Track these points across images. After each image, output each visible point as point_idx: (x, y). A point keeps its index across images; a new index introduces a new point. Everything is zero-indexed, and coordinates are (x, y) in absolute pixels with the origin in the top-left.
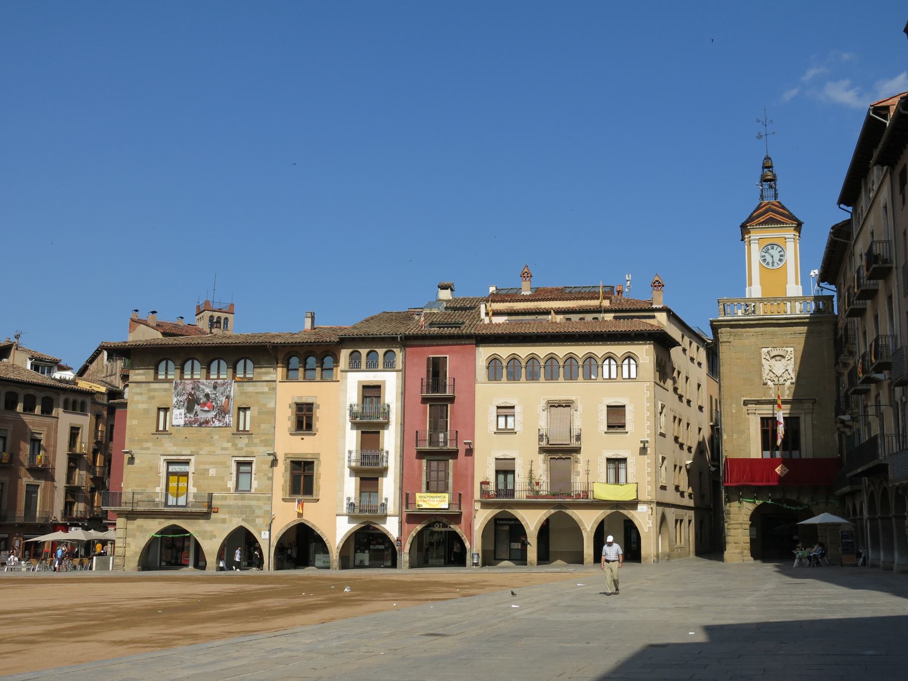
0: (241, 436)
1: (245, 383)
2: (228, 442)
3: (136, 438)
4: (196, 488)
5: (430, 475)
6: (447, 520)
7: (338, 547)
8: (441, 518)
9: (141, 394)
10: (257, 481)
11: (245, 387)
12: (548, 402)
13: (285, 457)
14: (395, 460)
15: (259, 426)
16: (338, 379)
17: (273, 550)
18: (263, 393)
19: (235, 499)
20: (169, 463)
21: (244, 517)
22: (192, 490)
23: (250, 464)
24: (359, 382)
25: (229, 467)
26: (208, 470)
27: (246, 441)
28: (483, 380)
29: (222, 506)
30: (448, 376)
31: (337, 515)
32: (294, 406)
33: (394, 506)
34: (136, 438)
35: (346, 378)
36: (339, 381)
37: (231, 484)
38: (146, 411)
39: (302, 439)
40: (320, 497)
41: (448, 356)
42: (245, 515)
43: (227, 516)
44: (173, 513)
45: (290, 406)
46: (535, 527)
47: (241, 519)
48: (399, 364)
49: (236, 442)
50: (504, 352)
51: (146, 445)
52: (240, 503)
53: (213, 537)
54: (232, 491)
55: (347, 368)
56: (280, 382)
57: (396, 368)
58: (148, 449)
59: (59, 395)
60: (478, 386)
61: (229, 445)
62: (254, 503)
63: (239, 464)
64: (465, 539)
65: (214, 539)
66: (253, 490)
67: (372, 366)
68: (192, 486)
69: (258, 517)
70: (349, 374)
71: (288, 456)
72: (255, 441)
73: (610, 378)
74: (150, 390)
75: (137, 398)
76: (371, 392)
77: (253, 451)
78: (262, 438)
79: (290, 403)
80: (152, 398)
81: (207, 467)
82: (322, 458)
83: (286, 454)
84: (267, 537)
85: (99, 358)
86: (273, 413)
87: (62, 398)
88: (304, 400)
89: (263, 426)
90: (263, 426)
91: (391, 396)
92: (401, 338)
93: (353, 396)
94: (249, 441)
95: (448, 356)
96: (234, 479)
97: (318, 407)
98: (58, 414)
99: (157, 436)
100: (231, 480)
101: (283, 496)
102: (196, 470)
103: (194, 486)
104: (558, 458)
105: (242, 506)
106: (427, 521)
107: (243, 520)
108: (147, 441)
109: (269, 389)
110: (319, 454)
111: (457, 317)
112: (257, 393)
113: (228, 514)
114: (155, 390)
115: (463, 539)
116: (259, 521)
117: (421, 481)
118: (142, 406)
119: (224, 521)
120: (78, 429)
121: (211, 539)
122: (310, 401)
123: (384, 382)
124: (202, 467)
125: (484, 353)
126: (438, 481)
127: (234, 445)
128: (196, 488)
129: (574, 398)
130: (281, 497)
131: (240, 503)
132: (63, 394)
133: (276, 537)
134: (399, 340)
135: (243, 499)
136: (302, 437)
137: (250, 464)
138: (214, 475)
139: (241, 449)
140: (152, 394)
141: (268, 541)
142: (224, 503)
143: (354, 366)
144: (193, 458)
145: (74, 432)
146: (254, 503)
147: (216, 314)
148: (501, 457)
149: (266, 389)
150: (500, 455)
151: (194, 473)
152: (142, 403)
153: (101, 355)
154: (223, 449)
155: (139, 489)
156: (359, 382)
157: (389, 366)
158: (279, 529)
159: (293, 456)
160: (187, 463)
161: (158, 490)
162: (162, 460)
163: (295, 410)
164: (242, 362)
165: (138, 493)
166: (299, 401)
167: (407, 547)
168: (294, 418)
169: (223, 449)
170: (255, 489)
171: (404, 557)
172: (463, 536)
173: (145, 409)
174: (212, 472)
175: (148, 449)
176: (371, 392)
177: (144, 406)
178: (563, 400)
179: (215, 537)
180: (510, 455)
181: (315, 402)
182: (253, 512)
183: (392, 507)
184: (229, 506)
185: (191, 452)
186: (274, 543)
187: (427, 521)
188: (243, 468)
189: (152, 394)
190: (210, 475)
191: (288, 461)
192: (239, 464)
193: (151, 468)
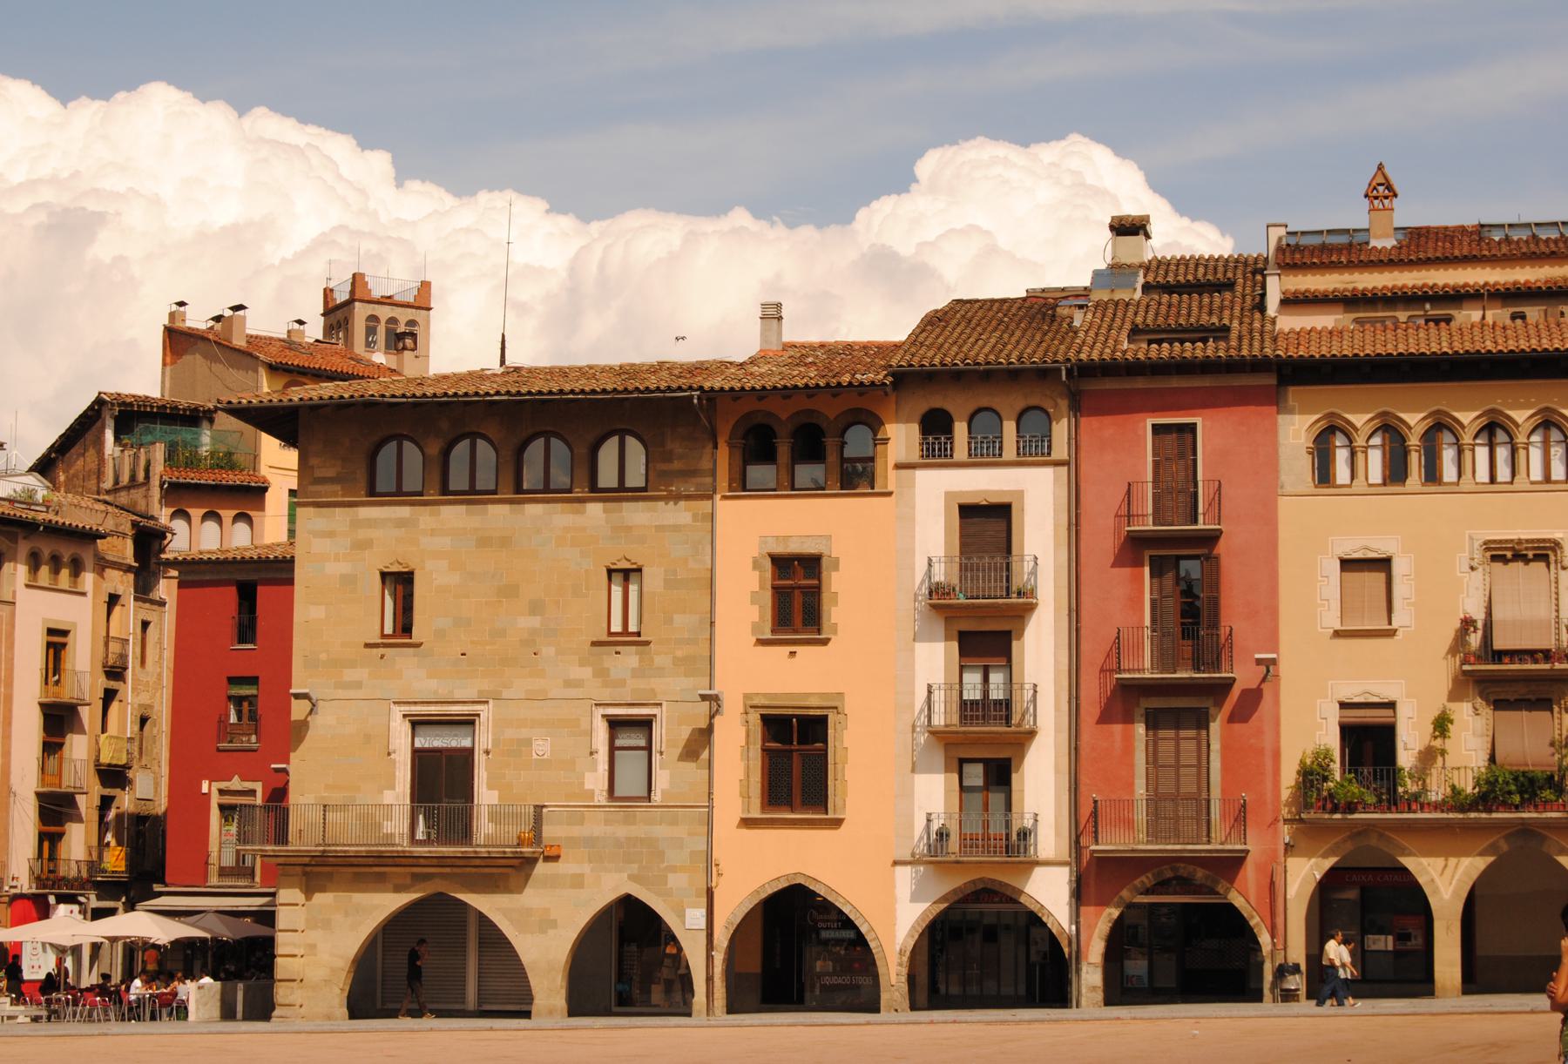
0: (618, 648)
1: (625, 505)
3: (323, 656)
4: (496, 793)
5: (1155, 752)
6: (1207, 872)
7: (901, 950)
8: (1191, 868)
9: (331, 534)
10: (668, 772)
11: (624, 514)
12: (1488, 546)
13: (745, 705)
14: (1057, 709)
15: (669, 621)
16: (890, 489)
17: (719, 957)
18: (676, 528)
19: (607, 822)
21: (636, 872)
23: (645, 724)
24: (949, 495)
25: (590, 733)
26: (528, 742)
28: (1301, 489)
29: (574, 842)
30: (1200, 477)
31: (895, 863)
32: (768, 564)
33: (1057, 834)
34: (323, 656)
35: (912, 484)
36: (890, 494)
37: (596, 781)
38: (348, 581)
39: (793, 654)
40: (848, 815)
41: (1198, 421)
42: (635, 866)
43: (586, 869)
44: (435, 862)
45: (756, 565)
46: (1454, 892)
47: (626, 875)
48: (1060, 449)
49: (606, 665)
51: (350, 675)
52: (622, 831)
53: (547, 924)
54: (601, 797)
55: (915, 456)
57: (1055, 456)
58: (358, 685)
59: (16, 543)
60: (1285, 506)
61: (586, 673)
62: (661, 831)
63: (615, 724)
64: (1257, 924)
65: (551, 932)
66: (657, 797)
67: (986, 453)
68: (485, 786)
69: (673, 869)
70: (920, 474)
71: (756, 702)
72: (659, 660)
73: (1547, 479)
74: (356, 524)
75: (320, 546)
77: (653, 690)
78: (679, 653)
79: (757, 555)
80: (362, 545)
81: (524, 733)
82: (849, 706)
83: (746, 696)
84: (702, 924)
85: (90, 436)
87: (24, 548)
88: (794, 548)
89: (678, 619)
90: (678, 619)
92: (1069, 372)
94: (641, 661)
95: (1198, 421)
96: (603, 766)
97: (836, 564)
98: (14, 592)
99: (382, 651)
100: (595, 770)
101: (743, 812)
102: (496, 742)
103: (490, 787)
104: (1516, 700)
105: (628, 839)
106: (1150, 875)
107: (632, 878)
108: (352, 664)
109: (695, 517)
110: (841, 694)
111: (1195, 310)
112: (660, 528)
113: (590, 861)
114: (371, 523)
115: (1252, 923)
116: (677, 881)
117: (1131, 766)
118: (336, 569)
119: (578, 882)
120: (65, 633)
121: (543, 931)
122: (809, 548)
123: (1020, 494)
124: (510, 733)
126: (1177, 766)
127: (601, 673)
128: (496, 793)
129: (1557, 535)
130: (737, 813)
131: (622, 831)
132: (25, 538)
133: (729, 923)
134: (1064, 378)
135: (628, 821)
136: (793, 649)
137: (645, 724)
138: (545, 757)
139: (622, 683)
140: (363, 534)
141: (703, 937)
142: (576, 831)
143: (934, 450)
145: (57, 642)
146: (661, 831)
147: (384, 313)
148: (1356, 700)
150: (1354, 693)
151: (487, 752)
152: (337, 559)
153: (99, 424)
154: (569, 684)
155: (335, 797)
157: (1034, 451)
158: (735, 901)
159: (767, 703)
160: (468, 722)
161: (388, 797)
162: (399, 716)
163: (769, 575)
164: (539, 443)
165: (337, 808)
166: (780, 549)
167: (1095, 950)
168: (767, 597)
169: (569, 684)
170: (663, 791)
171: (1090, 977)
172: (1252, 917)
173: (344, 577)
174: (542, 747)
175: (358, 685)
177: (344, 568)
178: (1527, 541)
179: (553, 924)
180: (1383, 692)
181: (825, 551)
182: (661, 855)
183: (1050, 839)
184: (590, 842)
185: (480, 692)
186: (722, 938)
187: (1150, 875)
188: (625, 739)
189: (363, 534)
190: (535, 756)
191: (755, 718)
192: (615, 724)
193: (368, 738)
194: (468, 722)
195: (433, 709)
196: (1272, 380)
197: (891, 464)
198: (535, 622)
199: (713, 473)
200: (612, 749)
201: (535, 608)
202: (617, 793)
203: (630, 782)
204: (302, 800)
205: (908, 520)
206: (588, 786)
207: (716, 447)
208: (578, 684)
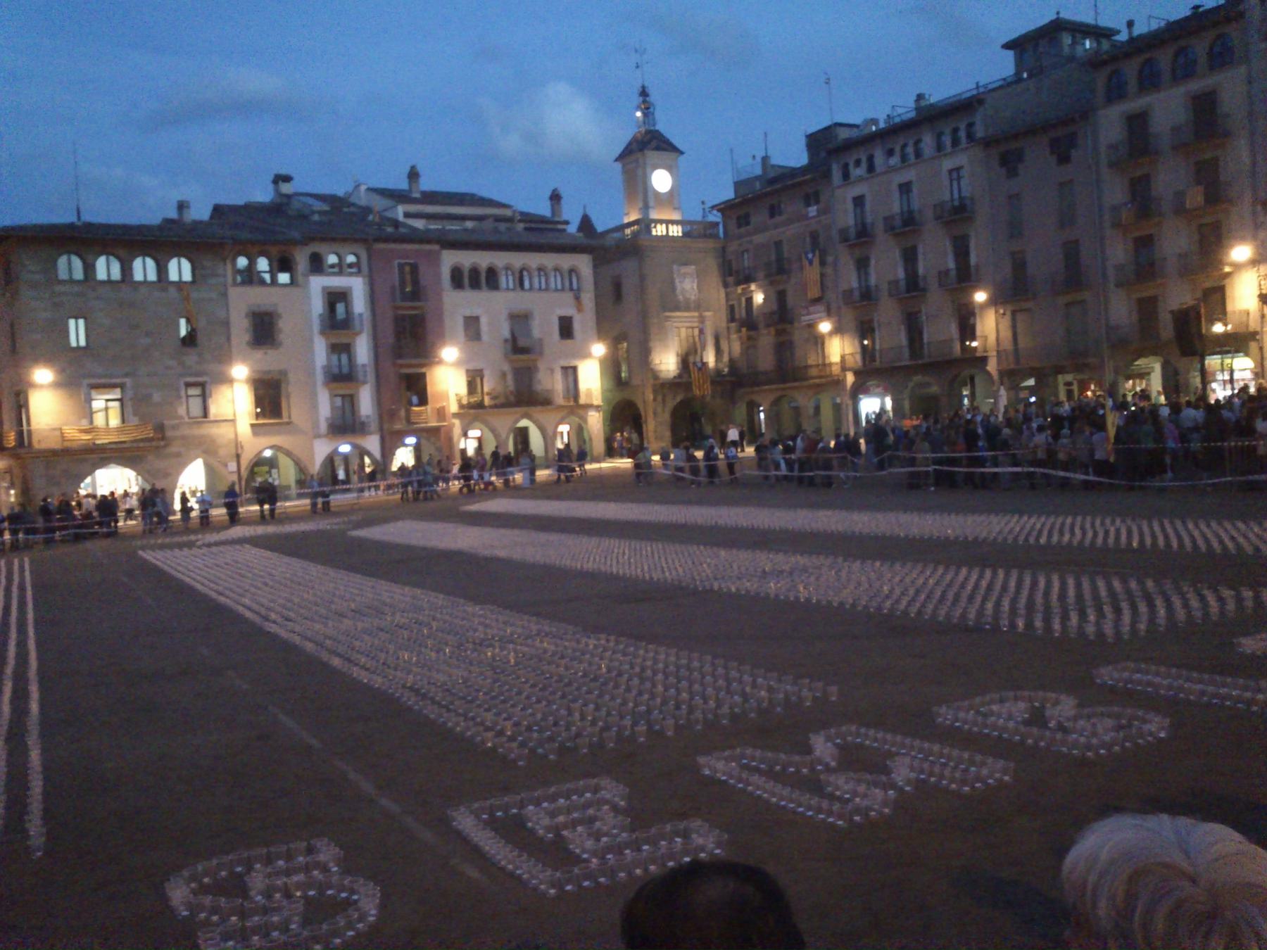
24: (324, 288)
25: (178, 390)
35: (307, 283)
50: (467, 259)
76: (335, 298)
86: (226, 324)
88: (263, 309)
91: (360, 304)
93: (317, 306)
97: (279, 316)
123: (350, 288)
125: (450, 259)
144: (128, 381)
149: (214, 295)
156: (324, 288)
166: (256, 309)
169: (168, 368)
188: (192, 391)
195: (103, 381)
196: (436, 247)
198: (148, 341)
199: (225, 276)
201: (148, 334)
202: (191, 415)
207: (225, 264)
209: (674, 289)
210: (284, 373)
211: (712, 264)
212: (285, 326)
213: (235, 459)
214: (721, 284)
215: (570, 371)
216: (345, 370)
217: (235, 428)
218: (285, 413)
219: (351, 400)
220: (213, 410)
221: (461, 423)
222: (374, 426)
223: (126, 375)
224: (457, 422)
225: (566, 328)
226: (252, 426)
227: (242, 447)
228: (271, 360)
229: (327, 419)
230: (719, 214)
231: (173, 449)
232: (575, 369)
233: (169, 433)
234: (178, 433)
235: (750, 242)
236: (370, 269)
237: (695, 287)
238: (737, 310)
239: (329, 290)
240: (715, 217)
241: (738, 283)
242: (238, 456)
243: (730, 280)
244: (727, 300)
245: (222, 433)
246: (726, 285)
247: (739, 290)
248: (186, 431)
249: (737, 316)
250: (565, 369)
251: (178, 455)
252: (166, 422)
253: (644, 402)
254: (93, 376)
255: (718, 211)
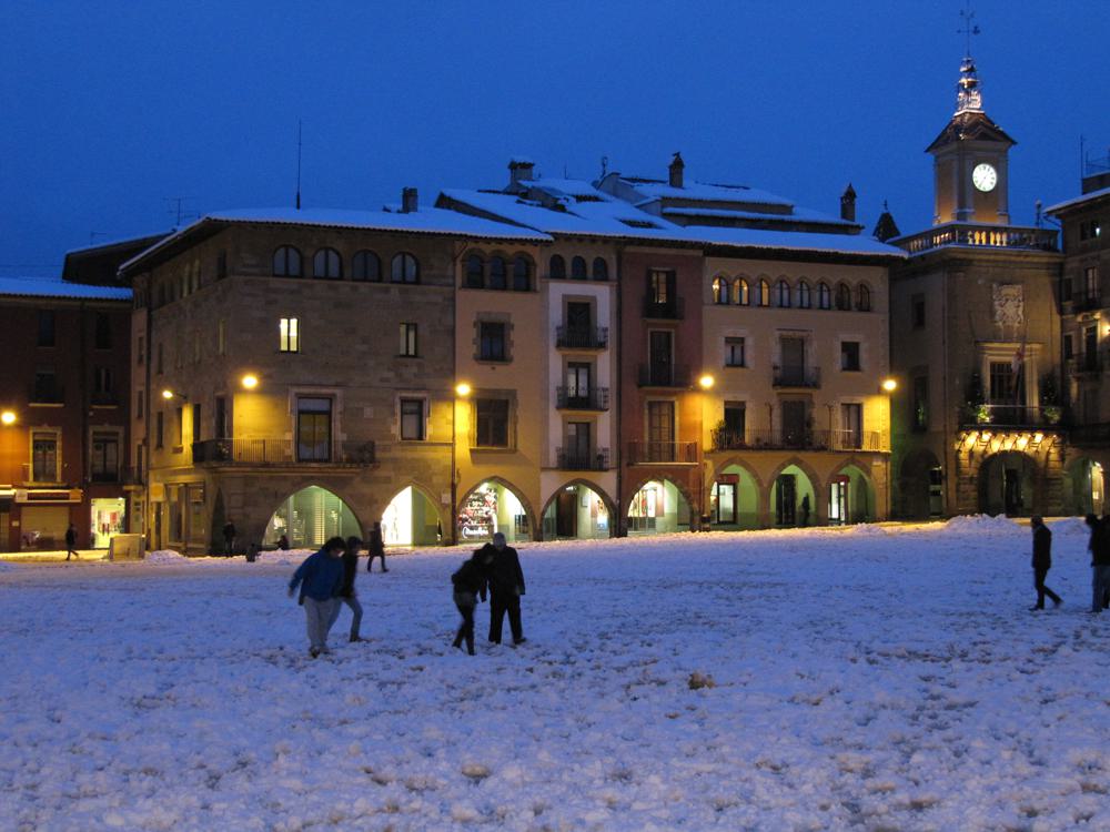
2: (389, 370)
20: (300, 397)
22: (340, 436)
24: (564, 296)
25: (393, 406)
26: (362, 409)
27: (415, 370)
35: (547, 289)
39: (493, 368)
43: (392, 474)
56: (460, 289)
61: (391, 375)
63: (404, 401)
67: (580, 275)
76: (579, 313)
91: (604, 316)
93: (556, 315)
96: (399, 423)
100: (396, 423)
103: (343, 431)
123: (594, 298)
144: (338, 392)
151: (341, 413)
156: (564, 296)
157: (601, 275)
160: (331, 399)
166: (486, 319)
169: (382, 380)
176: (579, 313)
188: (409, 407)
192: (404, 401)
194: (331, 399)
197: (538, 275)
198: (364, 348)
199: (454, 277)
200: (403, 413)
203: (411, 431)
204: (242, 438)
205: (545, 307)
206: (393, 432)
208: (387, 380)
209: (992, 313)
210: (513, 393)
211: (1044, 282)
212: (518, 339)
213: (450, 490)
214: (1054, 309)
215: (853, 409)
216: (582, 393)
217: (453, 452)
218: (510, 441)
219: (586, 430)
220: (430, 430)
221: (714, 465)
222: (611, 461)
223: (337, 385)
224: (710, 463)
225: (851, 354)
226: (472, 451)
227: (459, 476)
228: (500, 378)
229: (558, 450)
230: (1058, 221)
231: (381, 473)
232: (859, 408)
233: (378, 455)
234: (388, 455)
235: (1098, 257)
236: (619, 278)
237: (1020, 313)
238: (1074, 343)
239: (572, 300)
240: (1053, 225)
241: (1077, 310)
242: (453, 487)
243: (1068, 305)
244: (1062, 332)
245: (442, 455)
246: (1061, 311)
247: (1079, 319)
248: (397, 453)
249: (1075, 351)
250: (847, 406)
251: (388, 480)
252: (377, 443)
253: (946, 453)
254: (298, 385)
255: (1058, 217)
